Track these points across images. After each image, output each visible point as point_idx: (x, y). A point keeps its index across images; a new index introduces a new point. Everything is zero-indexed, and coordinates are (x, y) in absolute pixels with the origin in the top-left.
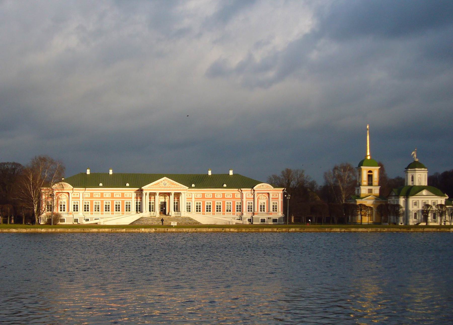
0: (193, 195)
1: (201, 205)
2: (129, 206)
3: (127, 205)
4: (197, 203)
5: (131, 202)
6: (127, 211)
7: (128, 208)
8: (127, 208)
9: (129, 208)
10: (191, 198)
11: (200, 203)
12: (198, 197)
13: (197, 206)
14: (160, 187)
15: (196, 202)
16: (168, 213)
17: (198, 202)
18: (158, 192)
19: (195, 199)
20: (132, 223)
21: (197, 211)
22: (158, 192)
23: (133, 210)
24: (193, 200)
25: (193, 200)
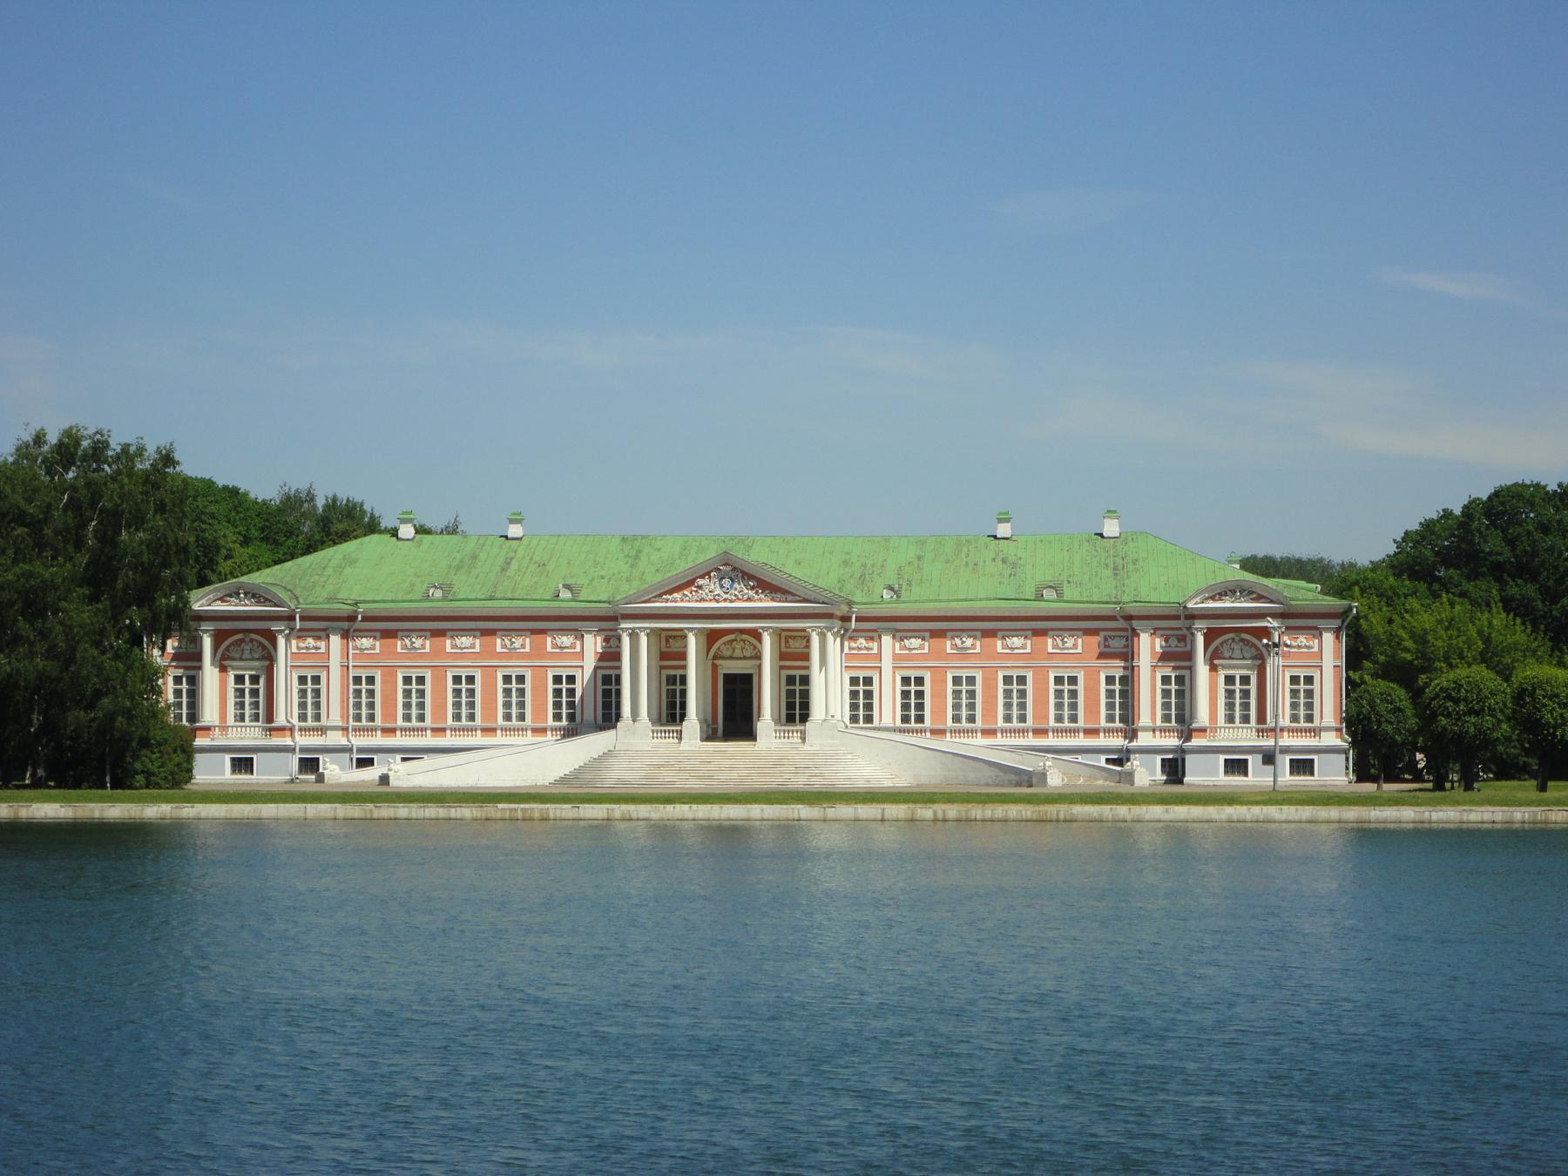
1: (927, 688)
3: (557, 693)
4: (906, 681)
13: (905, 694)
14: (702, 600)
17: (913, 674)
19: (896, 657)
20: (563, 780)
21: (905, 719)
24: (887, 663)
25: (887, 663)
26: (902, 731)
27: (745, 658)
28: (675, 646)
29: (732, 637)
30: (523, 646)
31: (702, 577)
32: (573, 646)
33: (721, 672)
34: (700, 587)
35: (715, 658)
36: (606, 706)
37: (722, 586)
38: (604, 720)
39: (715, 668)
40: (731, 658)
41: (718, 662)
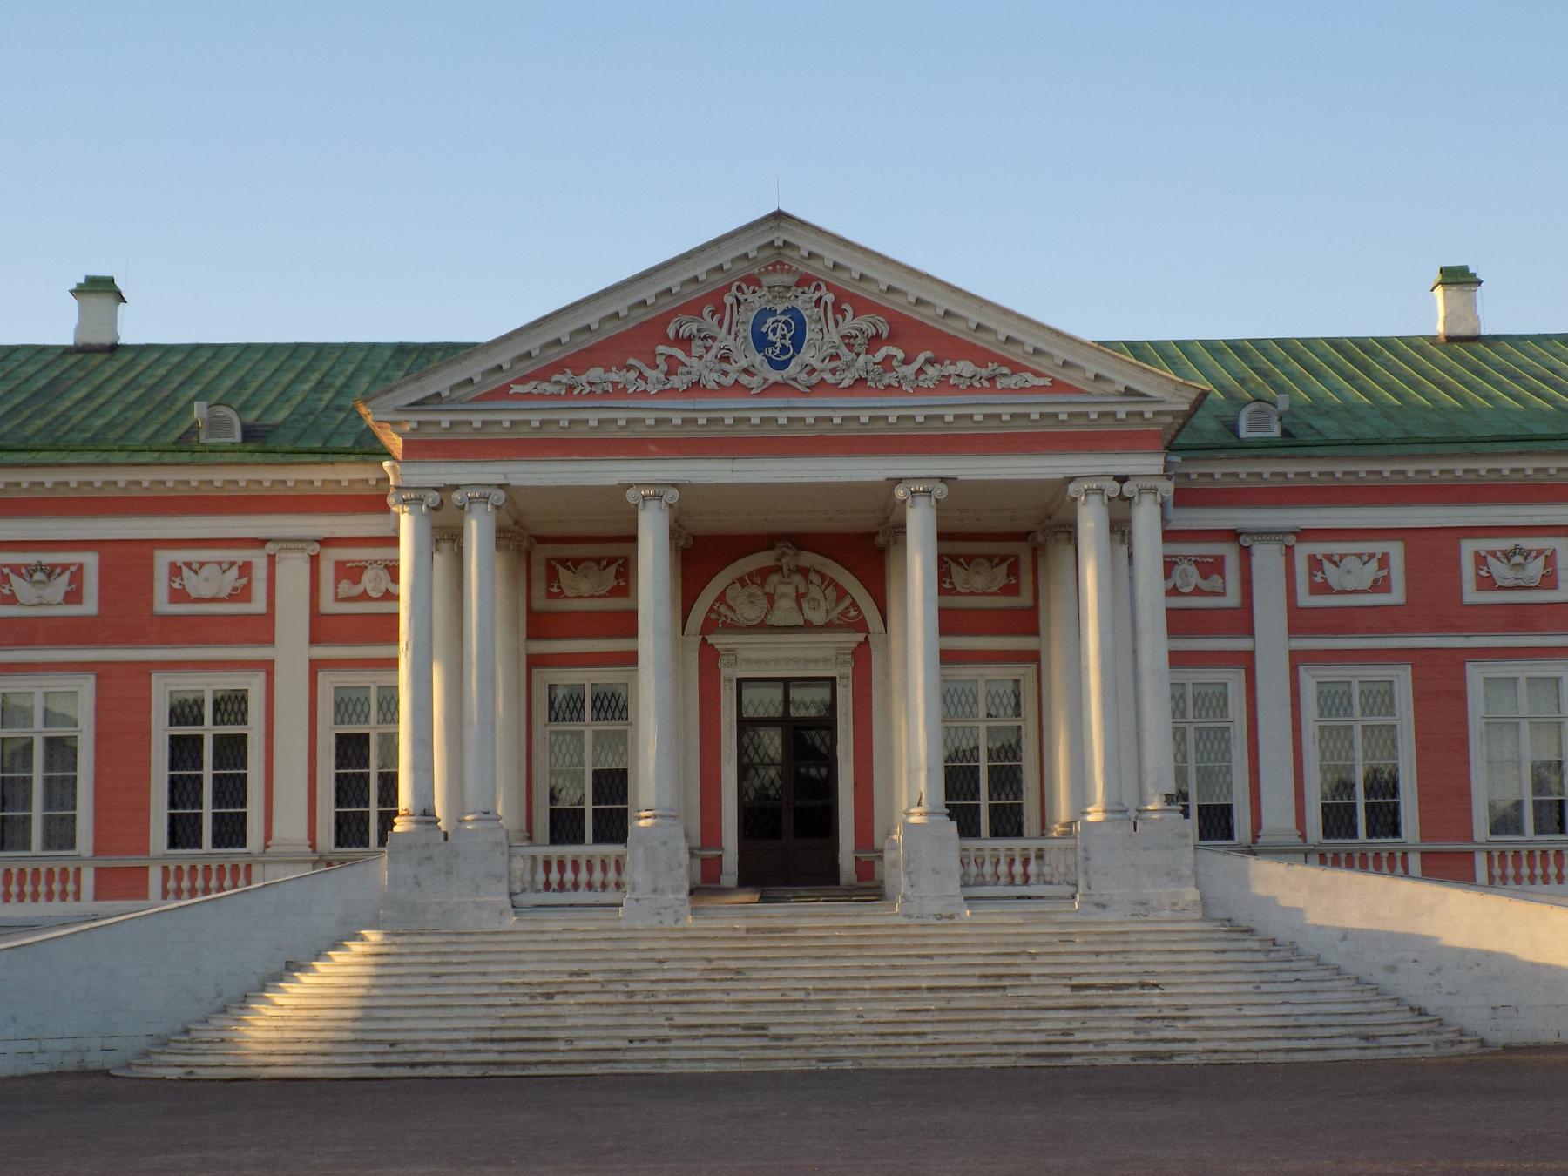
0: (1267, 560)
2: (232, 750)
3: (184, 751)
5: (254, 685)
6: (182, 833)
7: (209, 796)
8: (182, 790)
9: (232, 790)
10: (1242, 620)
11: (1382, 698)
12: (1353, 577)
15: (1310, 678)
16: (866, 869)
18: (650, 494)
19: (1300, 621)
21: (1338, 820)
22: (650, 494)
23: (291, 825)
24: (1271, 639)
25: (1271, 639)
26: (1326, 859)
27: (807, 627)
28: (583, 593)
29: (763, 559)
30: (74, 596)
31: (693, 308)
32: (243, 594)
33: (729, 672)
34: (684, 342)
35: (708, 627)
36: (349, 789)
37: (761, 342)
38: (350, 831)
39: (709, 659)
40: (763, 627)
41: (711, 639)
